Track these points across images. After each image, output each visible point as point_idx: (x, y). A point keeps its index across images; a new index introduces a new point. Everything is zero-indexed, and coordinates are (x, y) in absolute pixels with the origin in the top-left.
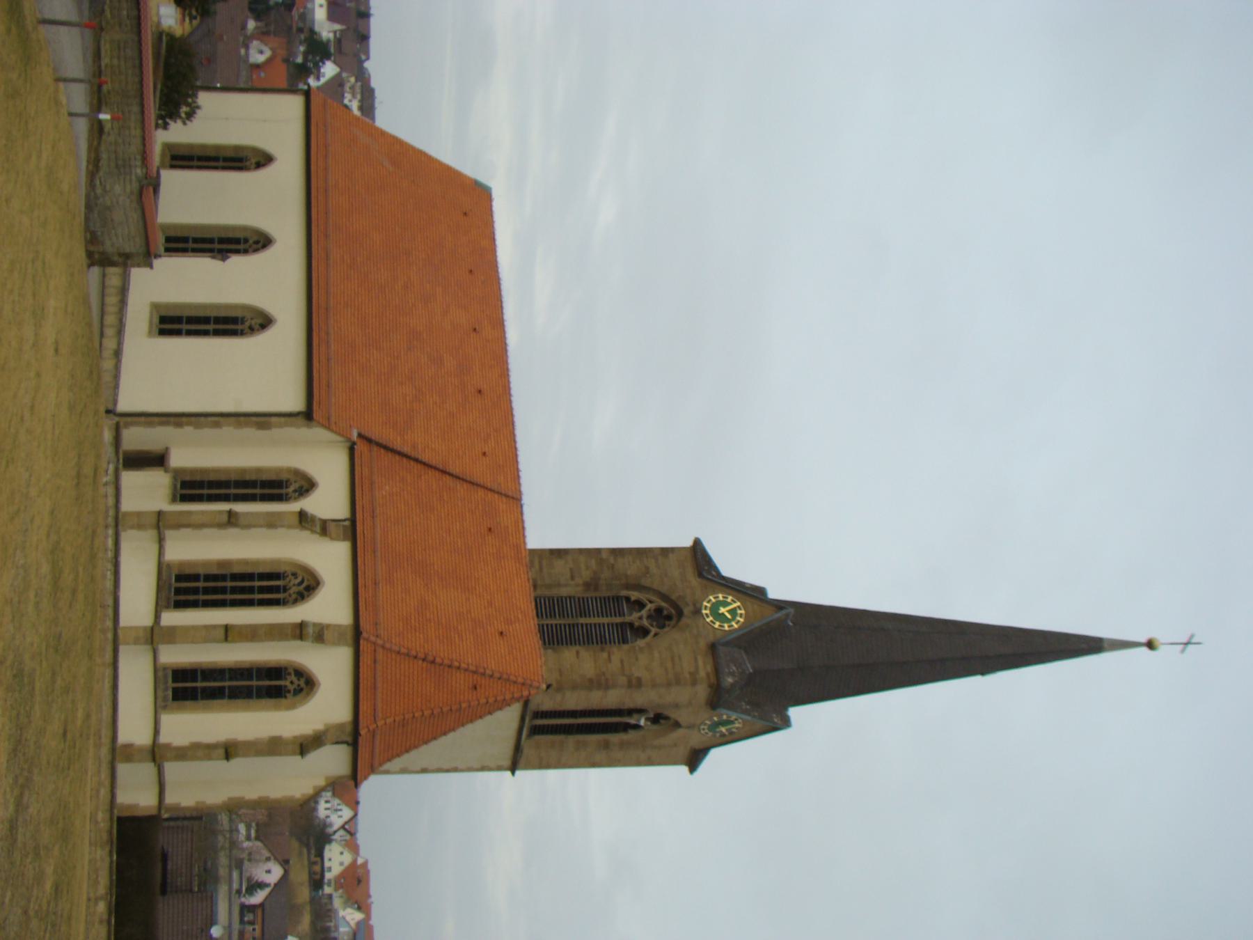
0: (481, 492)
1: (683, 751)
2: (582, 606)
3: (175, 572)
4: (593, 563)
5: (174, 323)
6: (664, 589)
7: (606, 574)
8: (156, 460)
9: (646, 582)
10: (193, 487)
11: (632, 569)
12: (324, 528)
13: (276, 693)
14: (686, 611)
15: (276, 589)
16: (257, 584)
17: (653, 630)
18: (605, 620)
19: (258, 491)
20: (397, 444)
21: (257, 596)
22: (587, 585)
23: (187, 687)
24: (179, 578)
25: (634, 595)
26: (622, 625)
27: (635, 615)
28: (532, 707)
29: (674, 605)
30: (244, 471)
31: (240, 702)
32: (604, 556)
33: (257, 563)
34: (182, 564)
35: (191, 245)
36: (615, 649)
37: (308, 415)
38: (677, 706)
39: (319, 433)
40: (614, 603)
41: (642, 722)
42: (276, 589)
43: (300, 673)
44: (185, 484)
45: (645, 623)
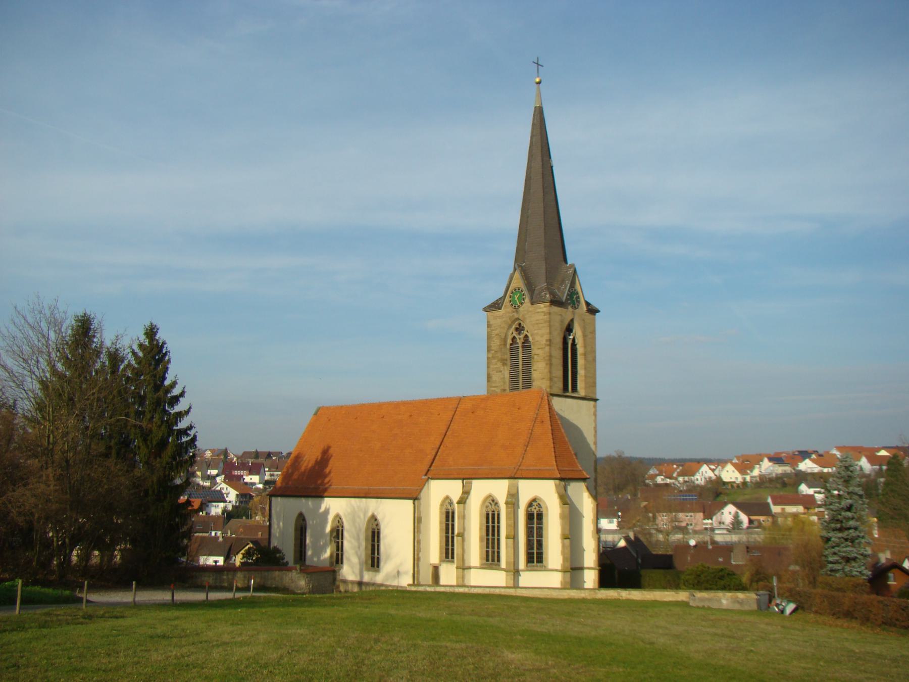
0: (456, 417)
1: (589, 316)
2: (514, 366)
3: (484, 561)
4: (494, 361)
5: (374, 561)
6: (506, 327)
7: (499, 355)
8: (436, 569)
9: (503, 336)
10: (448, 553)
11: (496, 343)
12: (466, 493)
13: (540, 516)
14: (516, 316)
15: (493, 515)
16: (490, 524)
17: (525, 332)
18: (521, 355)
19: (450, 523)
20: (430, 457)
21: (496, 524)
22: (504, 364)
23: (536, 557)
24: (487, 560)
25: (509, 341)
26: (523, 347)
27: (518, 341)
28: (560, 392)
29: (513, 322)
30: (441, 529)
31: (544, 533)
32: (490, 356)
33: (481, 524)
34: (481, 558)
35: (340, 553)
36: (533, 352)
37: (415, 499)
38: (562, 322)
39: (423, 495)
40: (513, 349)
41: (571, 337)
42: (493, 515)
43: (530, 505)
44: (447, 557)
45: (522, 336)
